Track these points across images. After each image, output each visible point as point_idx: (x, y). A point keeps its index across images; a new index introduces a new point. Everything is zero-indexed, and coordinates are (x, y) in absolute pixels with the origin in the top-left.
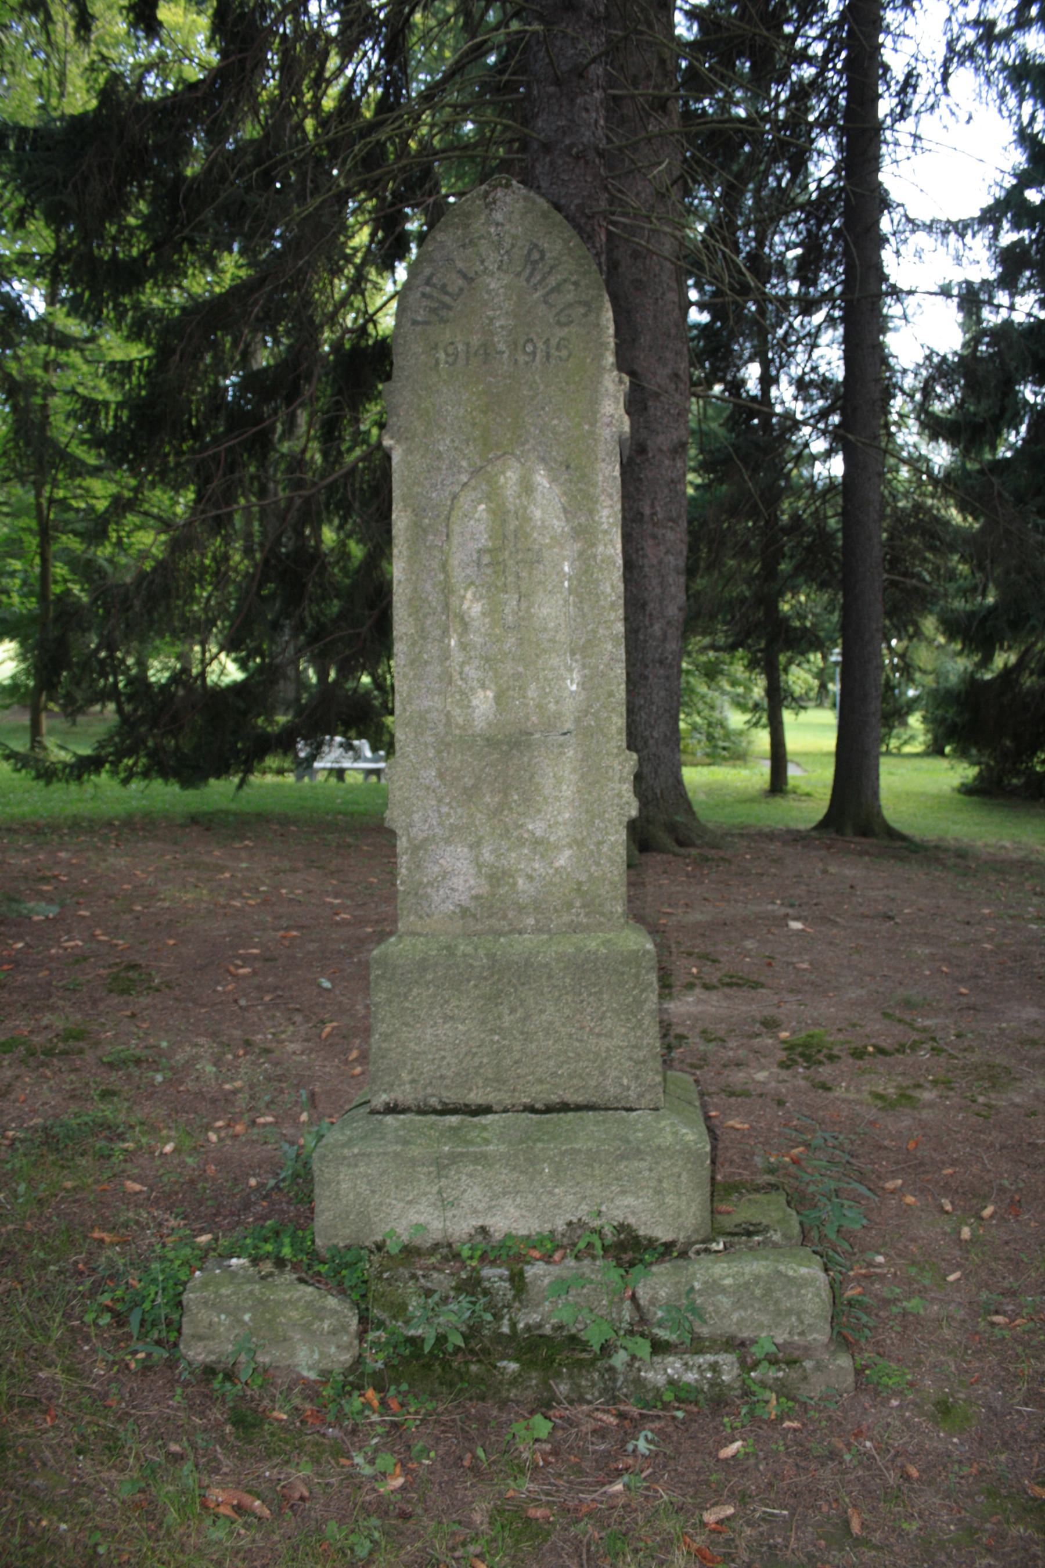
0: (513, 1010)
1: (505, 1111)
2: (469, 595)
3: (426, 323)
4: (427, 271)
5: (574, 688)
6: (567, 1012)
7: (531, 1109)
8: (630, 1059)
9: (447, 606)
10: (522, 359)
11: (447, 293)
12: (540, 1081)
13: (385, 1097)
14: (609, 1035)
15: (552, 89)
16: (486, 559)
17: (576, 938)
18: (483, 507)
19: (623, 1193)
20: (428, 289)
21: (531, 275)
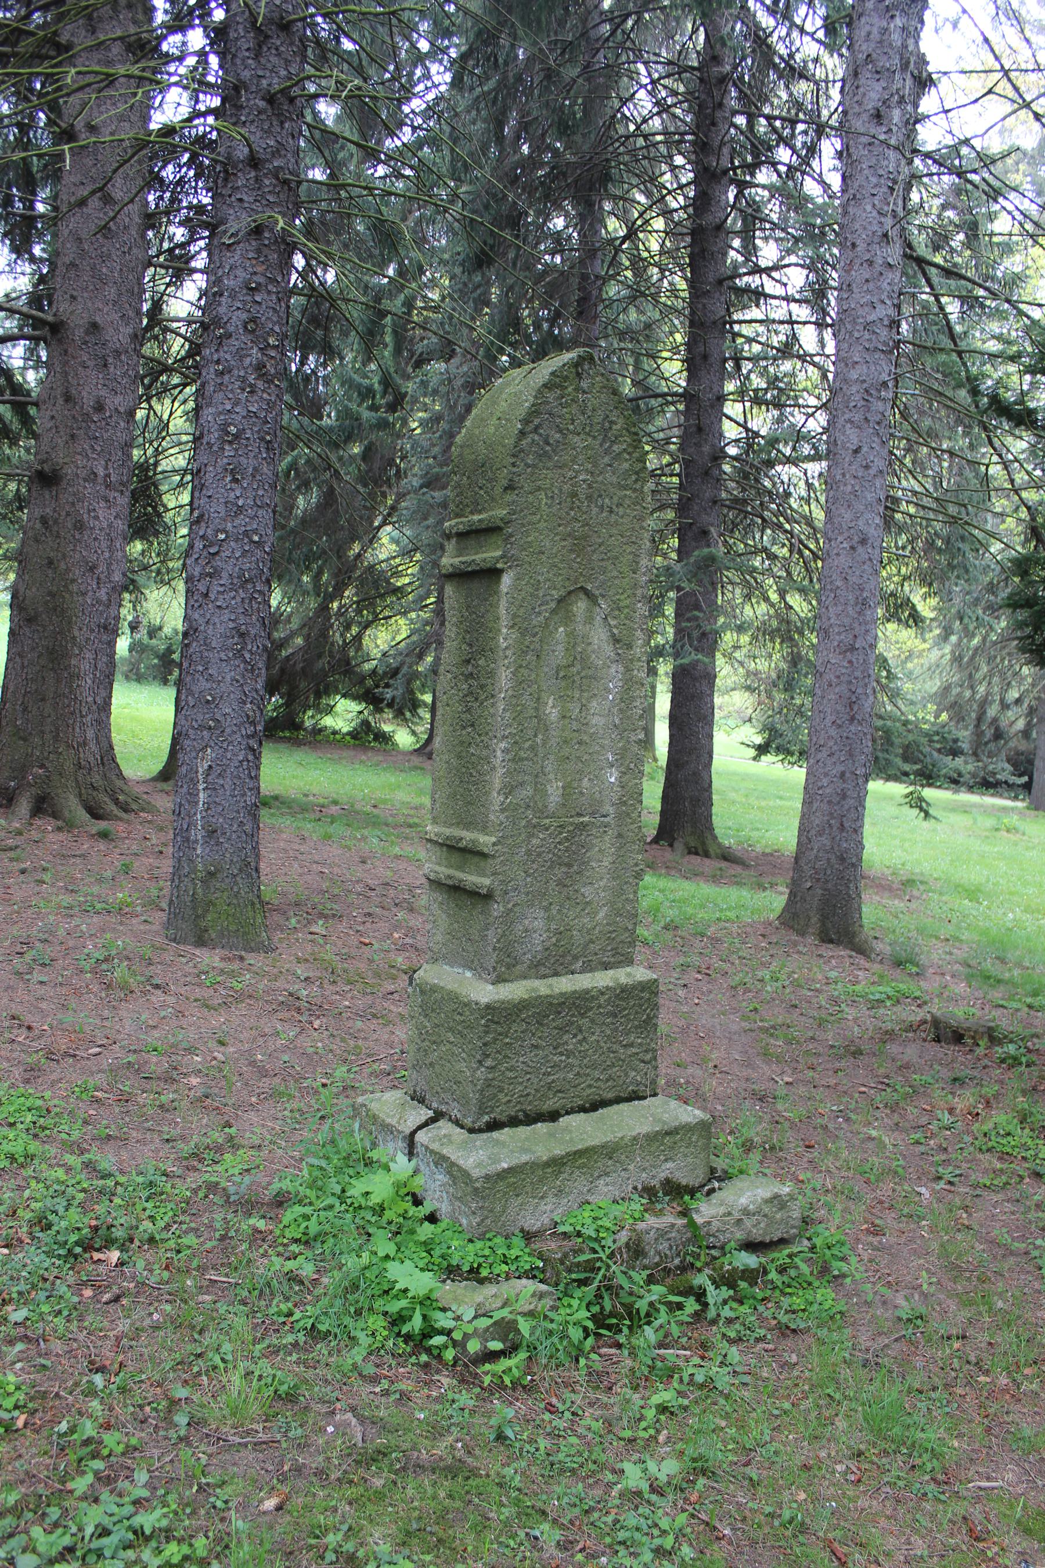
0: (575, 1036)
1: (568, 1113)
2: (550, 703)
3: (534, 466)
4: (536, 421)
5: (613, 780)
6: (609, 1032)
7: (583, 1109)
8: (643, 1061)
9: (537, 709)
10: (595, 510)
11: (548, 444)
12: (590, 1086)
13: (486, 1118)
14: (632, 1045)
15: (262, 104)
16: (562, 674)
17: (611, 972)
18: (561, 629)
19: (666, 1160)
20: (536, 438)
21: (604, 441)
